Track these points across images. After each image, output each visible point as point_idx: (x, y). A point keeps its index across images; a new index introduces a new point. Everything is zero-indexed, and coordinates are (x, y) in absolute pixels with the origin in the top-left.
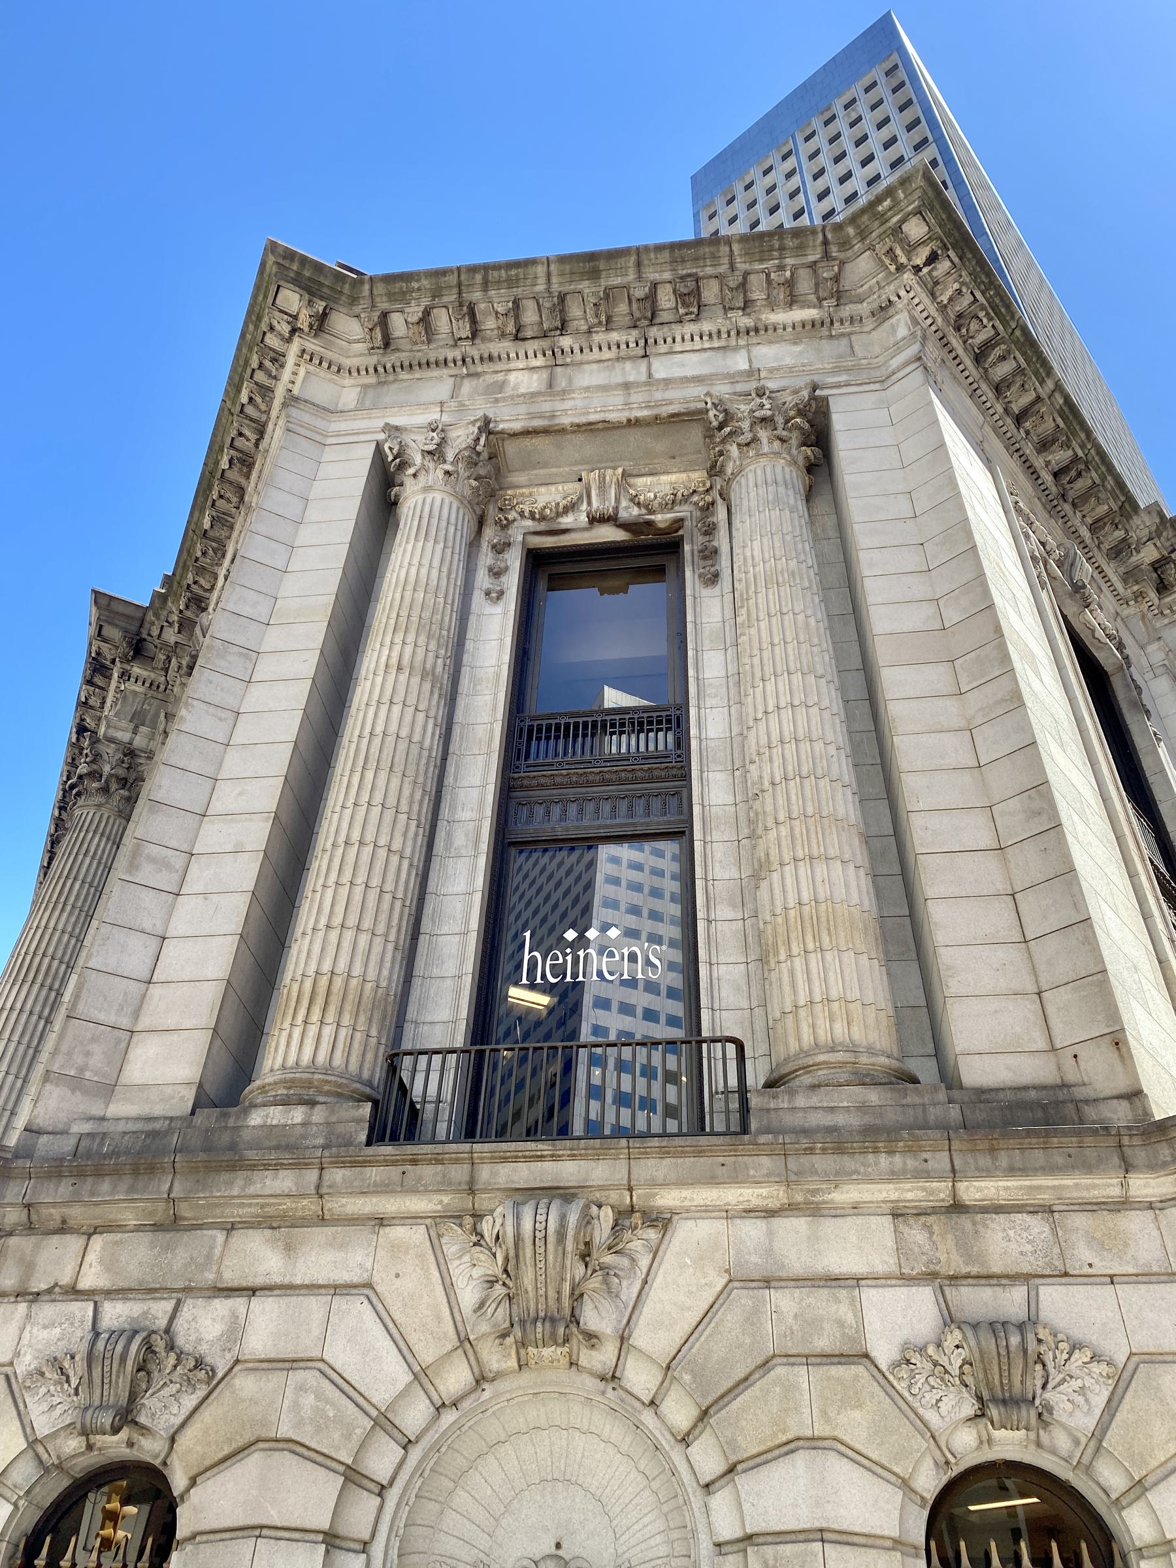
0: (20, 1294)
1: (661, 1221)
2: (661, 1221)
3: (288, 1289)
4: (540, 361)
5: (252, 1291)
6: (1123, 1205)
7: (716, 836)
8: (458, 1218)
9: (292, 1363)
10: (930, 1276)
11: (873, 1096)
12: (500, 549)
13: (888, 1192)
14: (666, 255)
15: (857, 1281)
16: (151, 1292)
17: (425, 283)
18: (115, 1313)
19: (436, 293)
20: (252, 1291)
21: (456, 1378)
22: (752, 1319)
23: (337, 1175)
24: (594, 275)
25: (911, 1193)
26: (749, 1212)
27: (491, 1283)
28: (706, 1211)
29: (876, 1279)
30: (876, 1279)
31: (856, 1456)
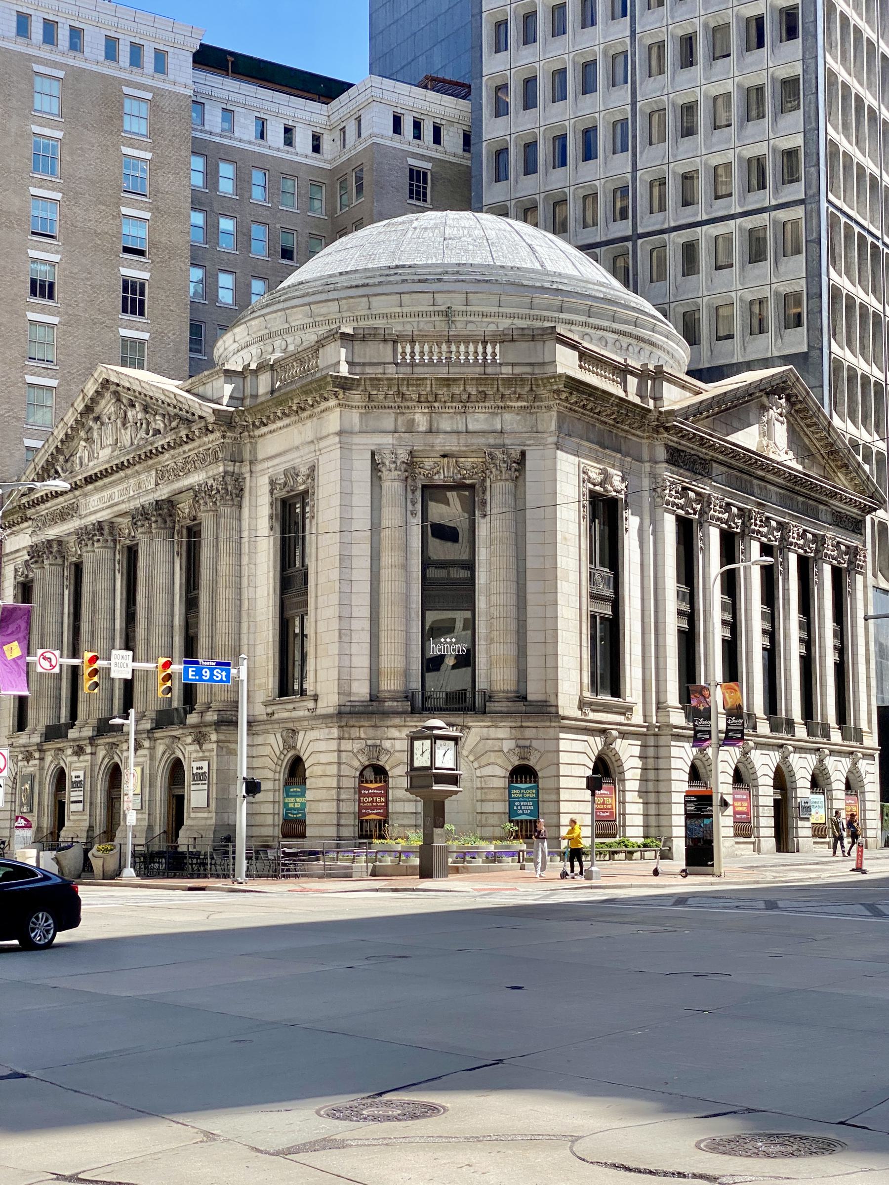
0: (350, 738)
1: (469, 728)
2: (469, 728)
4: (426, 410)
6: (550, 727)
7: (481, 618)
11: (509, 704)
12: (413, 492)
13: (510, 724)
14: (474, 382)
15: (502, 739)
16: (374, 739)
17: (385, 382)
18: (369, 742)
19: (389, 387)
22: (485, 744)
23: (408, 719)
24: (448, 386)
25: (514, 724)
26: (484, 727)
28: (477, 727)
29: (506, 739)
30: (506, 739)
31: (499, 766)
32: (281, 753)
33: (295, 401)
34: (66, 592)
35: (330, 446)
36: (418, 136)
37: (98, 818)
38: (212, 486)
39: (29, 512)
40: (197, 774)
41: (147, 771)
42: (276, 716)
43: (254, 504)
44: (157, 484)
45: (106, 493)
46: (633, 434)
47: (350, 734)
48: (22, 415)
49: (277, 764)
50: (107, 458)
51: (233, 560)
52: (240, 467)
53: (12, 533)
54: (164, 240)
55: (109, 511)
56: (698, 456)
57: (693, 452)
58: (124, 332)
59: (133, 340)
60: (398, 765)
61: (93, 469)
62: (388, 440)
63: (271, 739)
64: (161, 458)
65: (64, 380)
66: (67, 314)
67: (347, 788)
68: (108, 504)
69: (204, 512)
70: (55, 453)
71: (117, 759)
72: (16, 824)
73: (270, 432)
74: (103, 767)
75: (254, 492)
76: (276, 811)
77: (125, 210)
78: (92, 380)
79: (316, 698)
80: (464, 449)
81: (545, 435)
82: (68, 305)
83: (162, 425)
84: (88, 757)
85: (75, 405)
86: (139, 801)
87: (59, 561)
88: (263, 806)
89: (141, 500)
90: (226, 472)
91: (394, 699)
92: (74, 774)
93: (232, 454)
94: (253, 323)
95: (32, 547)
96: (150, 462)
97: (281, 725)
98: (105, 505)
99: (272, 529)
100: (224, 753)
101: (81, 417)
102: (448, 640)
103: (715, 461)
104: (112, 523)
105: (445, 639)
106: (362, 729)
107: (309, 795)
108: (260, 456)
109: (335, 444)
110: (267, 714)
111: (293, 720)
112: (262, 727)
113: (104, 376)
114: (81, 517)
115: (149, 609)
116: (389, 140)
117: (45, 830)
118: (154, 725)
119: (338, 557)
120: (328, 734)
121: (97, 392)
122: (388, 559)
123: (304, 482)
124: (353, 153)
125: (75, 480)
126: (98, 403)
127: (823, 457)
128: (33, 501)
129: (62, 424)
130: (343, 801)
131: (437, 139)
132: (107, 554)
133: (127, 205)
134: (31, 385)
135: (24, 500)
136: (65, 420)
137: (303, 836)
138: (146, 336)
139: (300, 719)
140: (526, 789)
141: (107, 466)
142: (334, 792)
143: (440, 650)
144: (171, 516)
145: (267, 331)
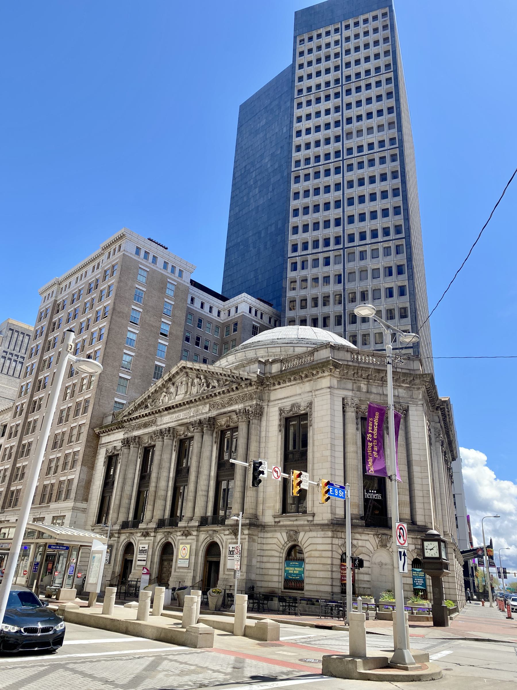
0: (337, 538)
3: (361, 540)
5: (358, 540)
8: (376, 535)
9: (363, 547)
10: (414, 544)
11: (410, 526)
20: (358, 540)
21: (376, 549)
23: (365, 530)
25: (413, 536)
27: (379, 541)
32: (285, 543)
33: (304, 373)
34: (139, 460)
35: (325, 393)
36: (256, 315)
37: (155, 569)
38: (248, 410)
39: (125, 424)
40: (142, 550)
41: (194, 547)
42: (281, 523)
43: (268, 420)
44: (209, 410)
45: (175, 415)
47: (337, 535)
48: (116, 388)
49: (282, 549)
50: (181, 399)
51: (258, 444)
52: (262, 403)
53: (108, 435)
54: (174, 332)
55: (176, 423)
58: (157, 363)
59: (160, 366)
60: (360, 554)
61: (171, 403)
62: (350, 394)
63: (278, 535)
64: (214, 399)
65: (133, 377)
66: (138, 352)
67: (336, 565)
68: (176, 419)
69: (241, 422)
70: (147, 398)
71: (170, 540)
72: (143, 572)
73: (281, 388)
74: (160, 544)
75: (268, 414)
76: (280, 574)
77: (163, 320)
78: (176, 367)
79: (314, 515)
80: (383, 402)
81: (417, 400)
82: (139, 349)
83: (217, 384)
84: (152, 538)
85: (164, 377)
86: (188, 563)
87: (138, 446)
88: (270, 570)
89: (198, 417)
90: (257, 404)
91: (357, 519)
92: (141, 546)
93: (259, 397)
94: (239, 354)
95: (124, 439)
96: (207, 401)
97: (288, 528)
98: (174, 420)
99: (280, 431)
100: (251, 541)
101: (165, 383)
102: (373, 491)
104: (174, 428)
105: (371, 491)
106: (343, 533)
107: (307, 567)
108: (272, 398)
109: (328, 392)
110: (275, 522)
111: (297, 526)
112: (269, 529)
113: (183, 365)
114: (157, 426)
115: (198, 467)
116: (247, 315)
117: (116, 573)
118: (199, 524)
119: (330, 445)
120: (324, 535)
121: (177, 372)
122: (351, 448)
123: (304, 410)
124: (233, 317)
125: (159, 409)
126: (175, 377)
128: (131, 419)
129: (154, 385)
130: (334, 571)
131: (261, 318)
132: (170, 442)
133: (164, 318)
134: (121, 377)
135: (125, 418)
136: (157, 384)
137: (302, 589)
138: (164, 365)
139: (302, 526)
140: (419, 572)
141: (181, 402)
142: (329, 567)
143: (369, 496)
144: (214, 425)
145: (245, 358)
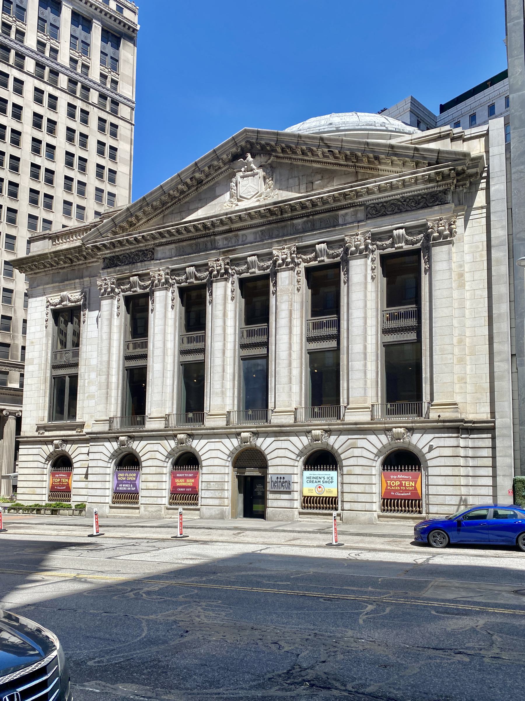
46: (89, 263)
56: (140, 251)
57: (133, 251)
103: (161, 245)
127: (347, 166)
